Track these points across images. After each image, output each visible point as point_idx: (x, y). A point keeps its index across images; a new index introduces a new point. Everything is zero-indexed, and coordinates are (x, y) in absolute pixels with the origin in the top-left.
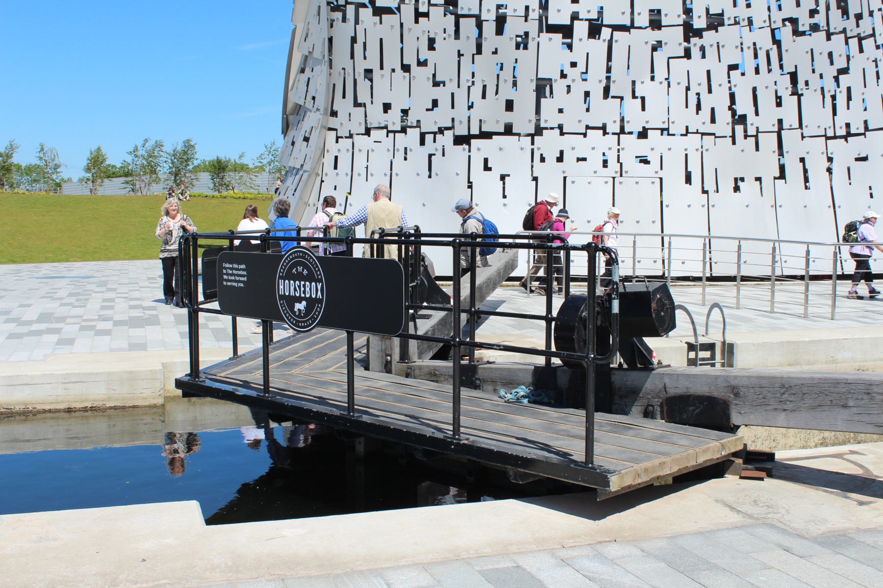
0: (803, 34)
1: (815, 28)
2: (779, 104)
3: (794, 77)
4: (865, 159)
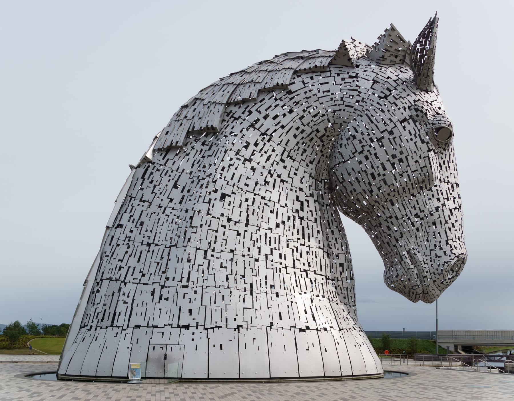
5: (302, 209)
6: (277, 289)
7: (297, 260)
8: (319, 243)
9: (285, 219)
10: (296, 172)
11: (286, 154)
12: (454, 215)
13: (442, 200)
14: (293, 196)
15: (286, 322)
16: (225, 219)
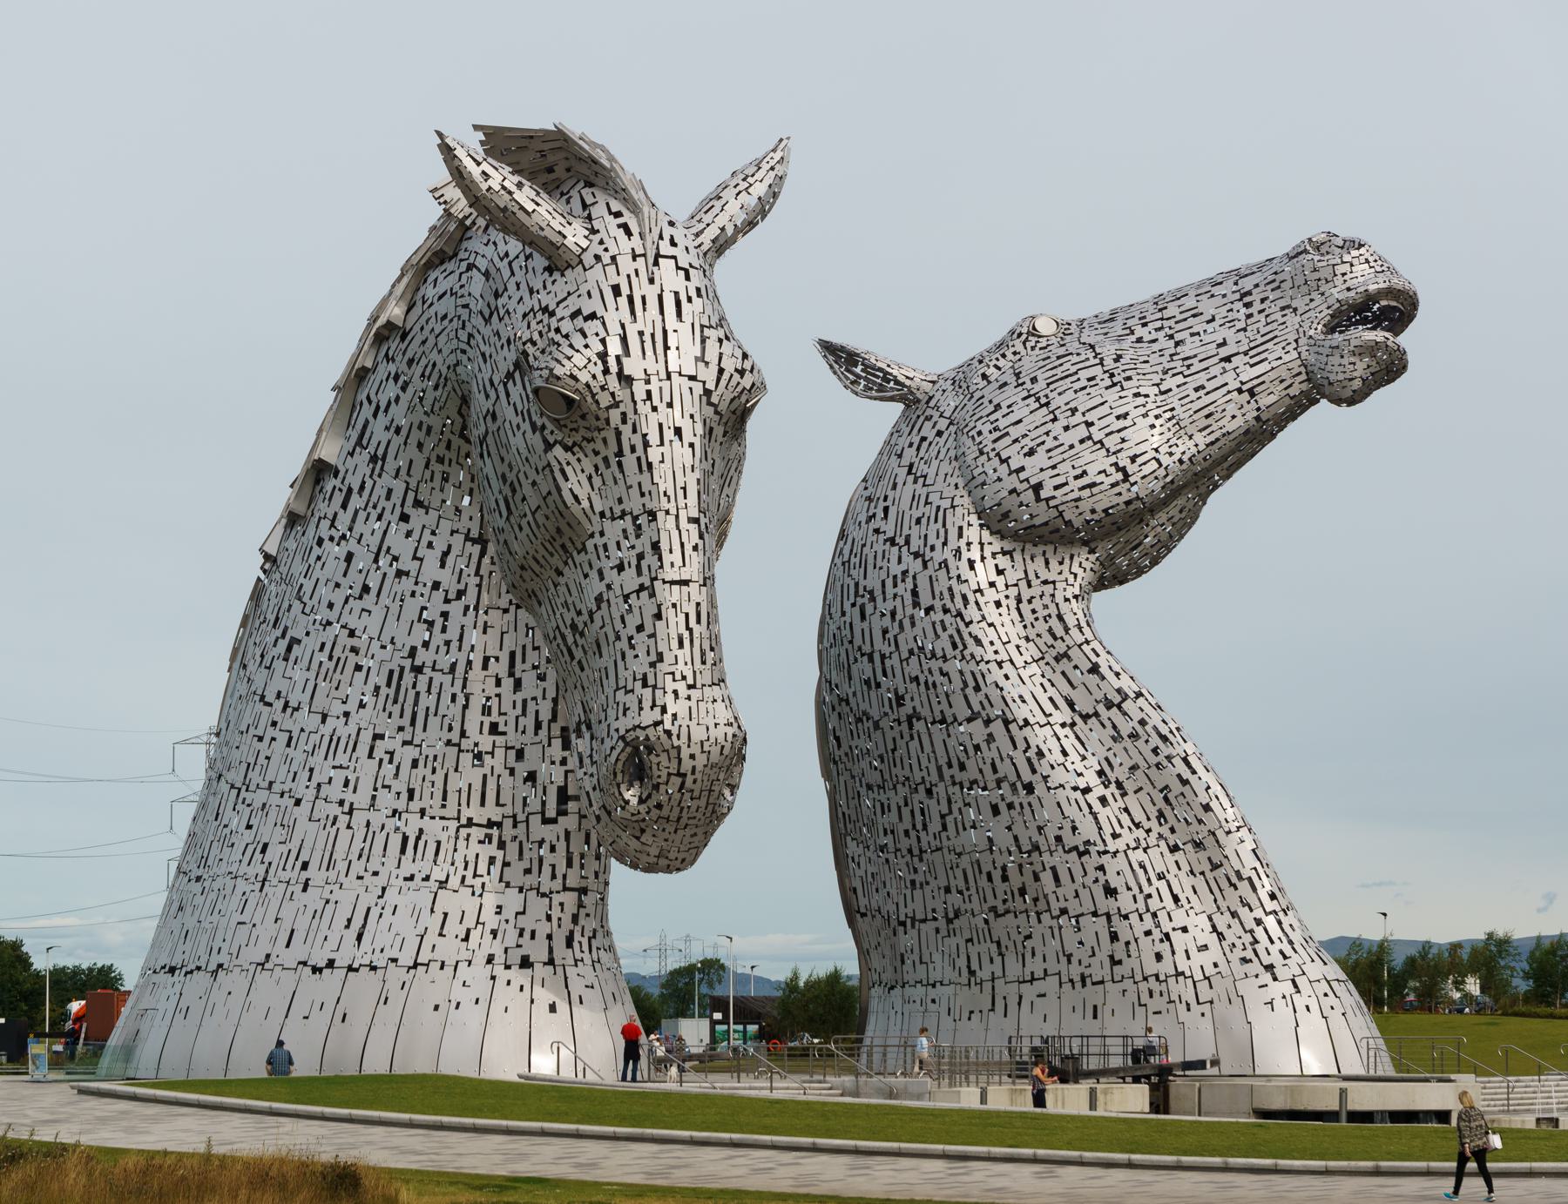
0: (1003, 915)
1: (1007, 912)
2: (992, 961)
3: (999, 943)
4: (1044, 995)
5: (426, 644)
6: (311, 872)
7: (384, 786)
8: (450, 729)
9: (382, 683)
10: (432, 538)
11: (411, 495)
12: (636, 611)
13: (606, 572)
14: (412, 607)
15: (298, 951)
16: (279, 704)
